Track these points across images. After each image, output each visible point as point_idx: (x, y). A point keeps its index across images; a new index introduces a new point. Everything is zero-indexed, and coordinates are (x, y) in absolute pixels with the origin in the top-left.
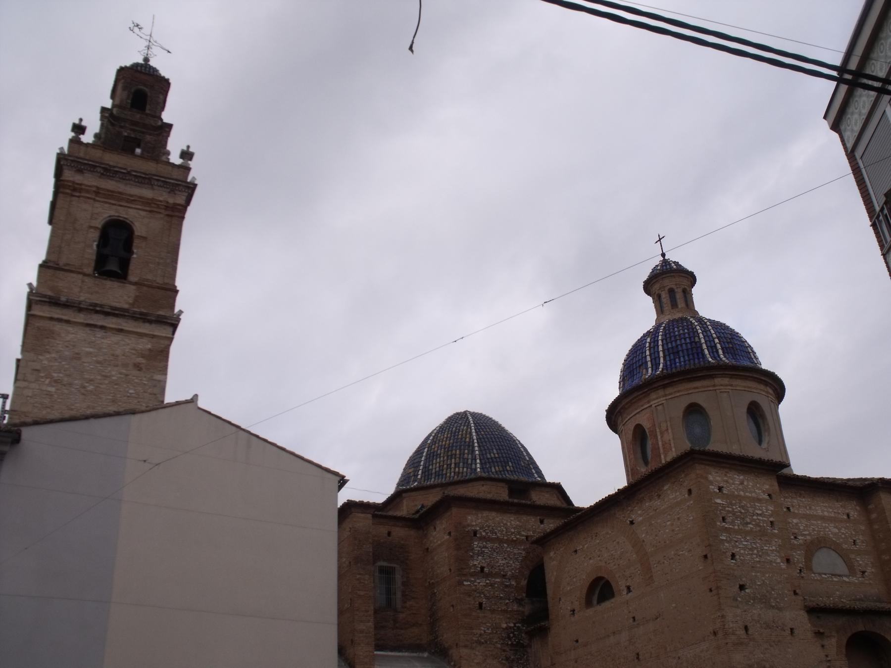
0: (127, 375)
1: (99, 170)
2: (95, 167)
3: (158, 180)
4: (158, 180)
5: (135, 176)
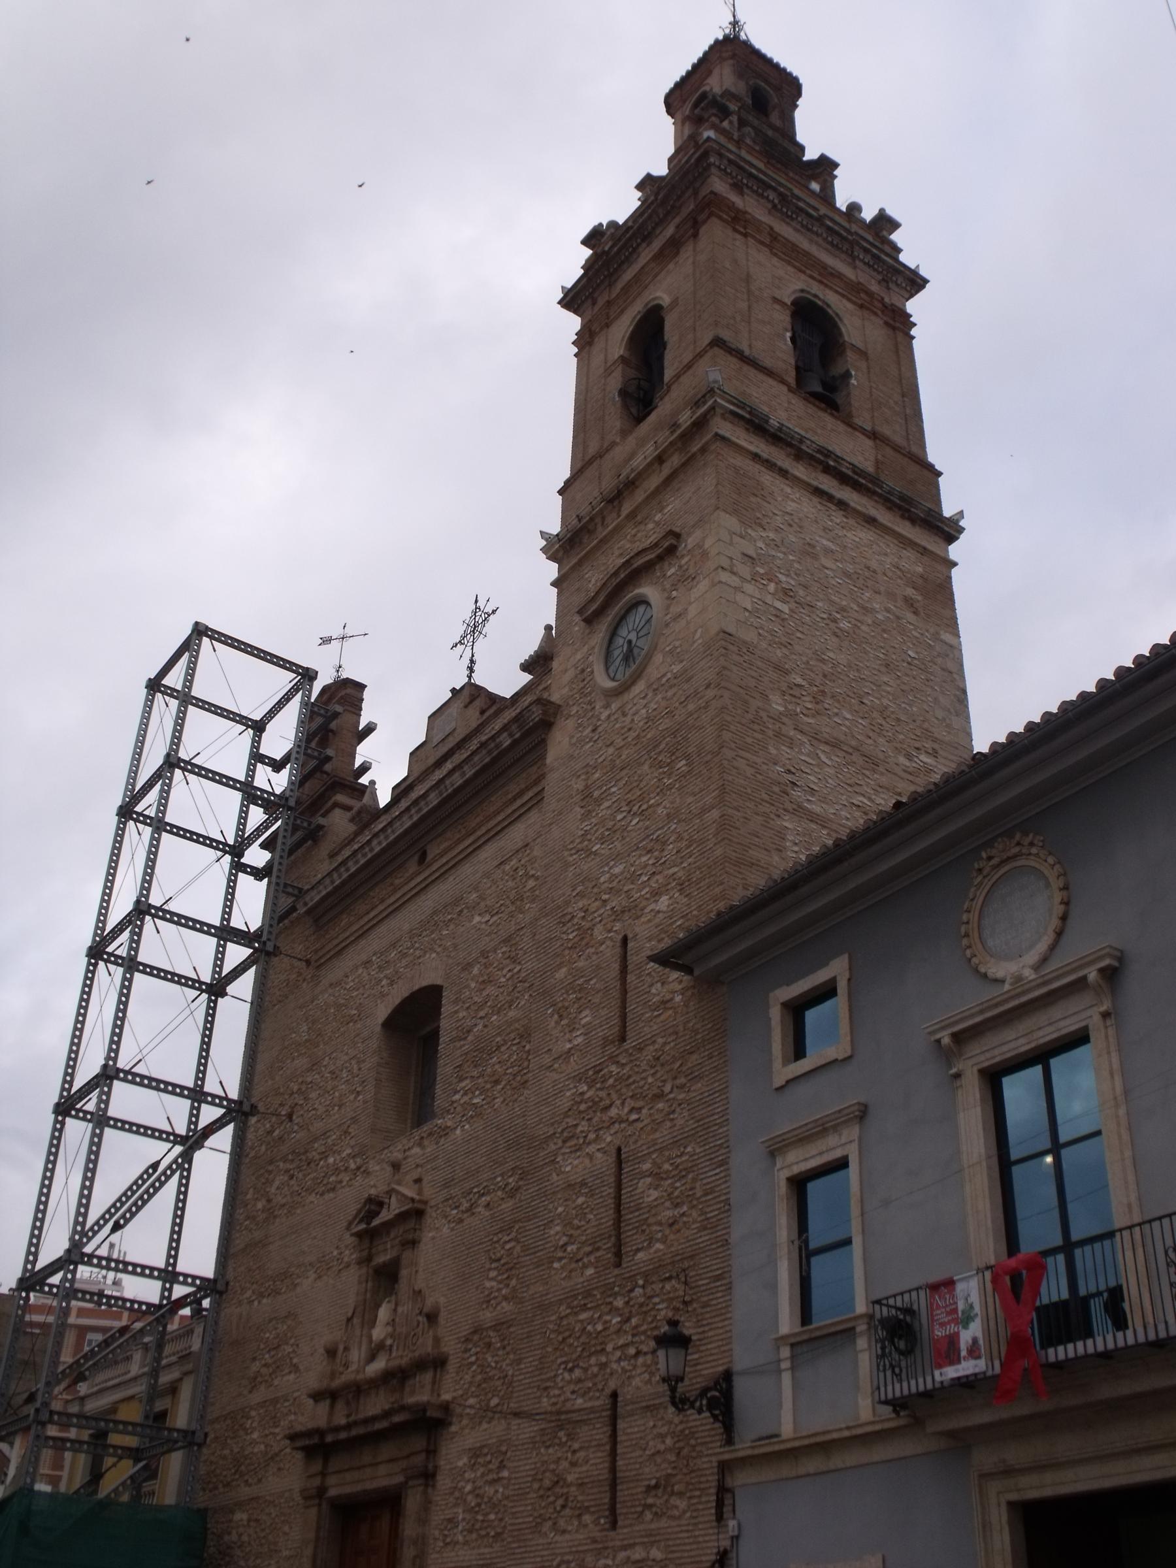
0: (898, 618)
1: (772, 196)
2: (768, 187)
3: (866, 251)
4: (866, 251)
5: (829, 229)
